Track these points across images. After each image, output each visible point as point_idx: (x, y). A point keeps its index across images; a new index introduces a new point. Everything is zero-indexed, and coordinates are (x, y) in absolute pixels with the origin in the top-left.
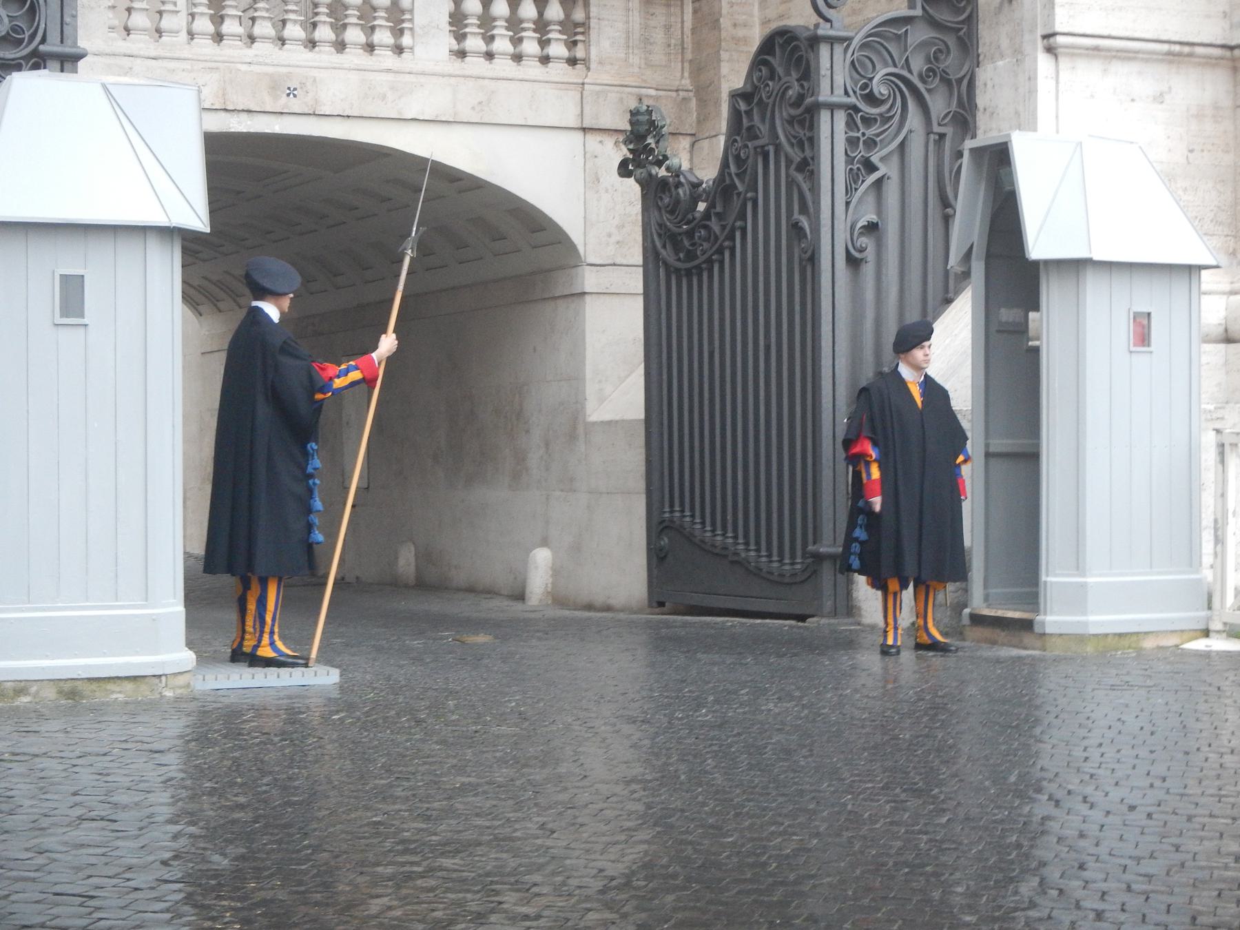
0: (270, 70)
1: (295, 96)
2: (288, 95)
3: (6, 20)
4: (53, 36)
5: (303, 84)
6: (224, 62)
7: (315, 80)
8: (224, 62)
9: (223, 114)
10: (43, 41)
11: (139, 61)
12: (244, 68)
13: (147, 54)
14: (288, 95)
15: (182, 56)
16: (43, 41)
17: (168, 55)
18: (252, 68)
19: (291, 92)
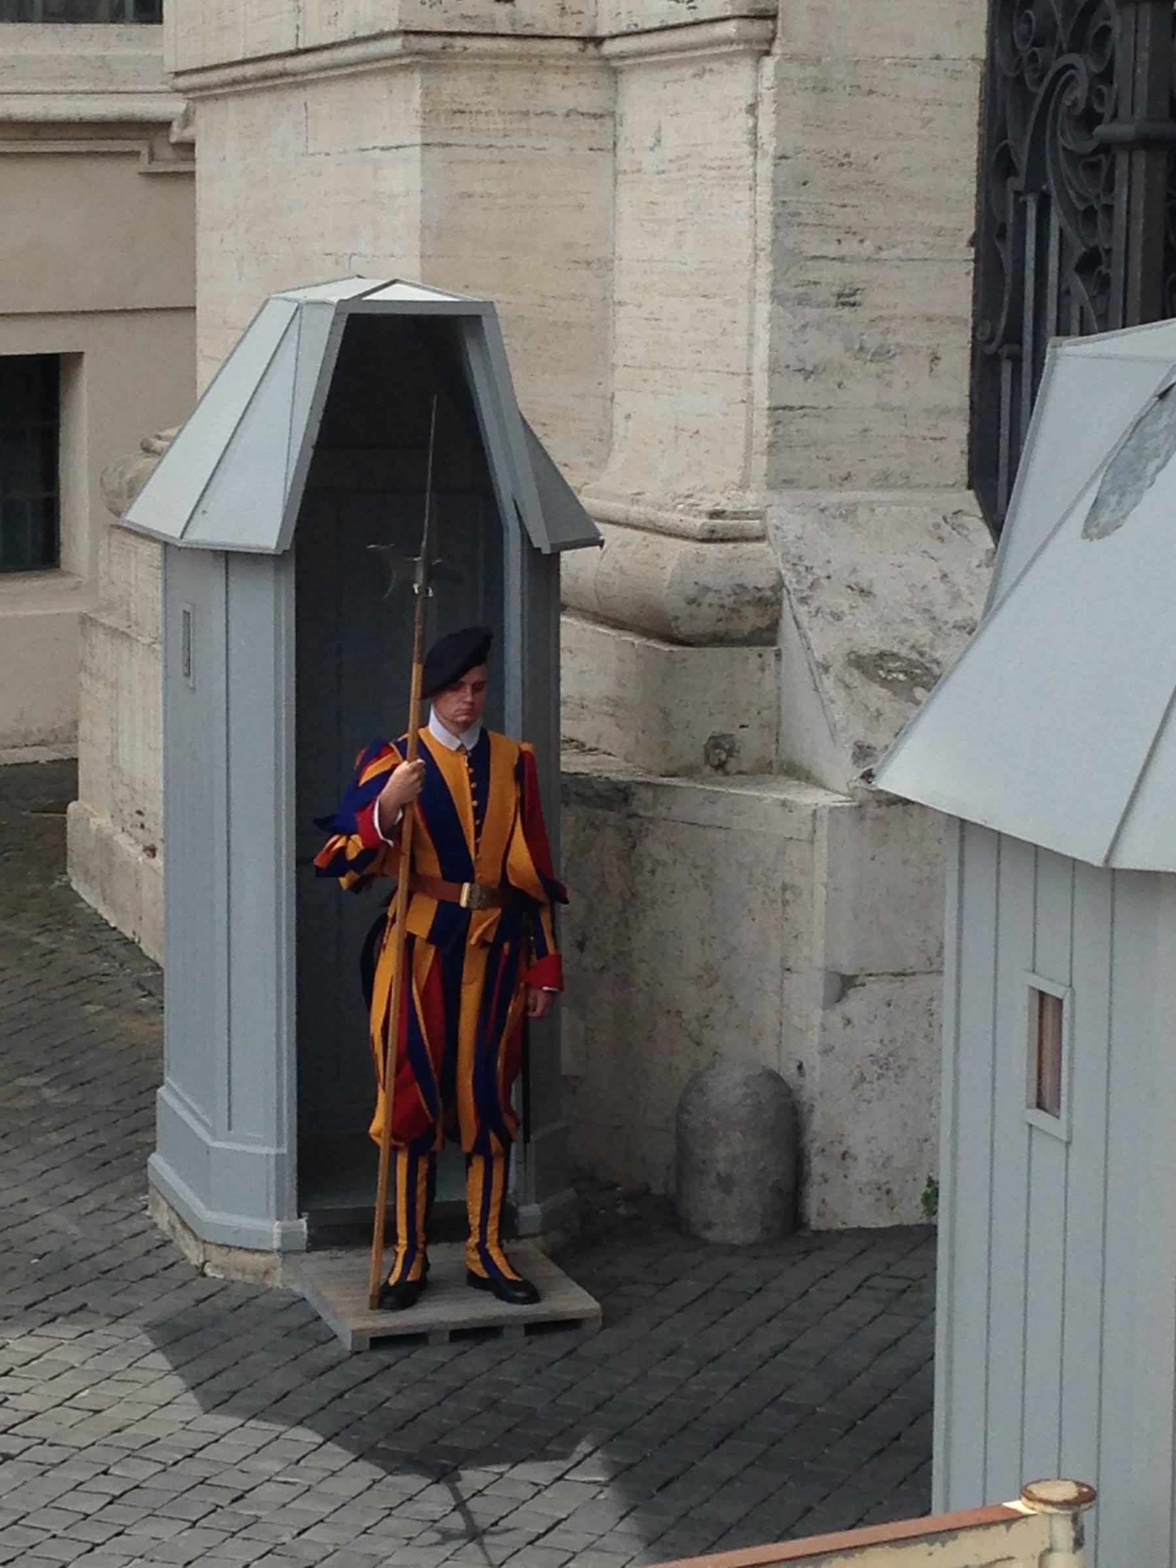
16: (1115, 116)
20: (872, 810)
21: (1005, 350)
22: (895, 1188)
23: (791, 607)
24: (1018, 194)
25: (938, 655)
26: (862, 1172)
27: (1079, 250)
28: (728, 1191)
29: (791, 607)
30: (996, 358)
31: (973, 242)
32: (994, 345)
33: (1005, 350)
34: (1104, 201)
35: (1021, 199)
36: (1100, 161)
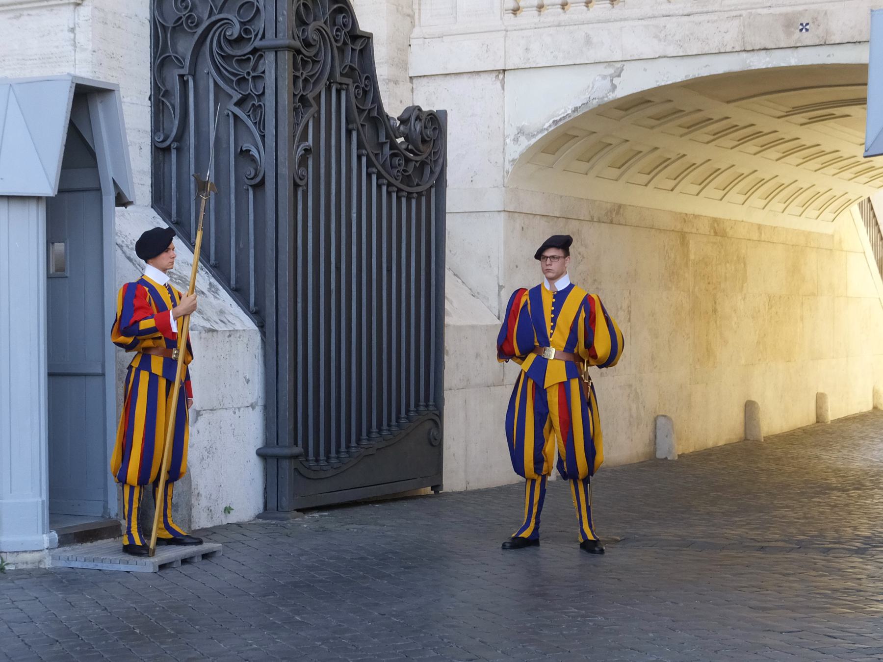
0: (789, 9)
1: (807, 30)
2: (801, 30)
3: (238, 26)
4: (270, 34)
5: (815, 20)
6: (746, 9)
7: (826, 13)
8: (746, 9)
9: (744, 55)
10: (263, 36)
11: (674, 19)
12: (765, 11)
13: (681, 12)
14: (801, 30)
15: (710, 10)
16: (263, 36)
17: (700, 10)
18: (772, 11)
19: (804, 27)
20: (204, 335)
21: (175, 145)
22: (212, 508)
23: (124, 252)
24: (181, 76)
25: (185, 273)
26: (204, 502)
27: (237, 97)
28: (176, 511)
29: (124, 252)
30: (168, 149)
31: (150, 99)
32: (167, 143)
33: (175, 145)
34: (252, 74)
35: (185, 78)
36: (249, 58)
